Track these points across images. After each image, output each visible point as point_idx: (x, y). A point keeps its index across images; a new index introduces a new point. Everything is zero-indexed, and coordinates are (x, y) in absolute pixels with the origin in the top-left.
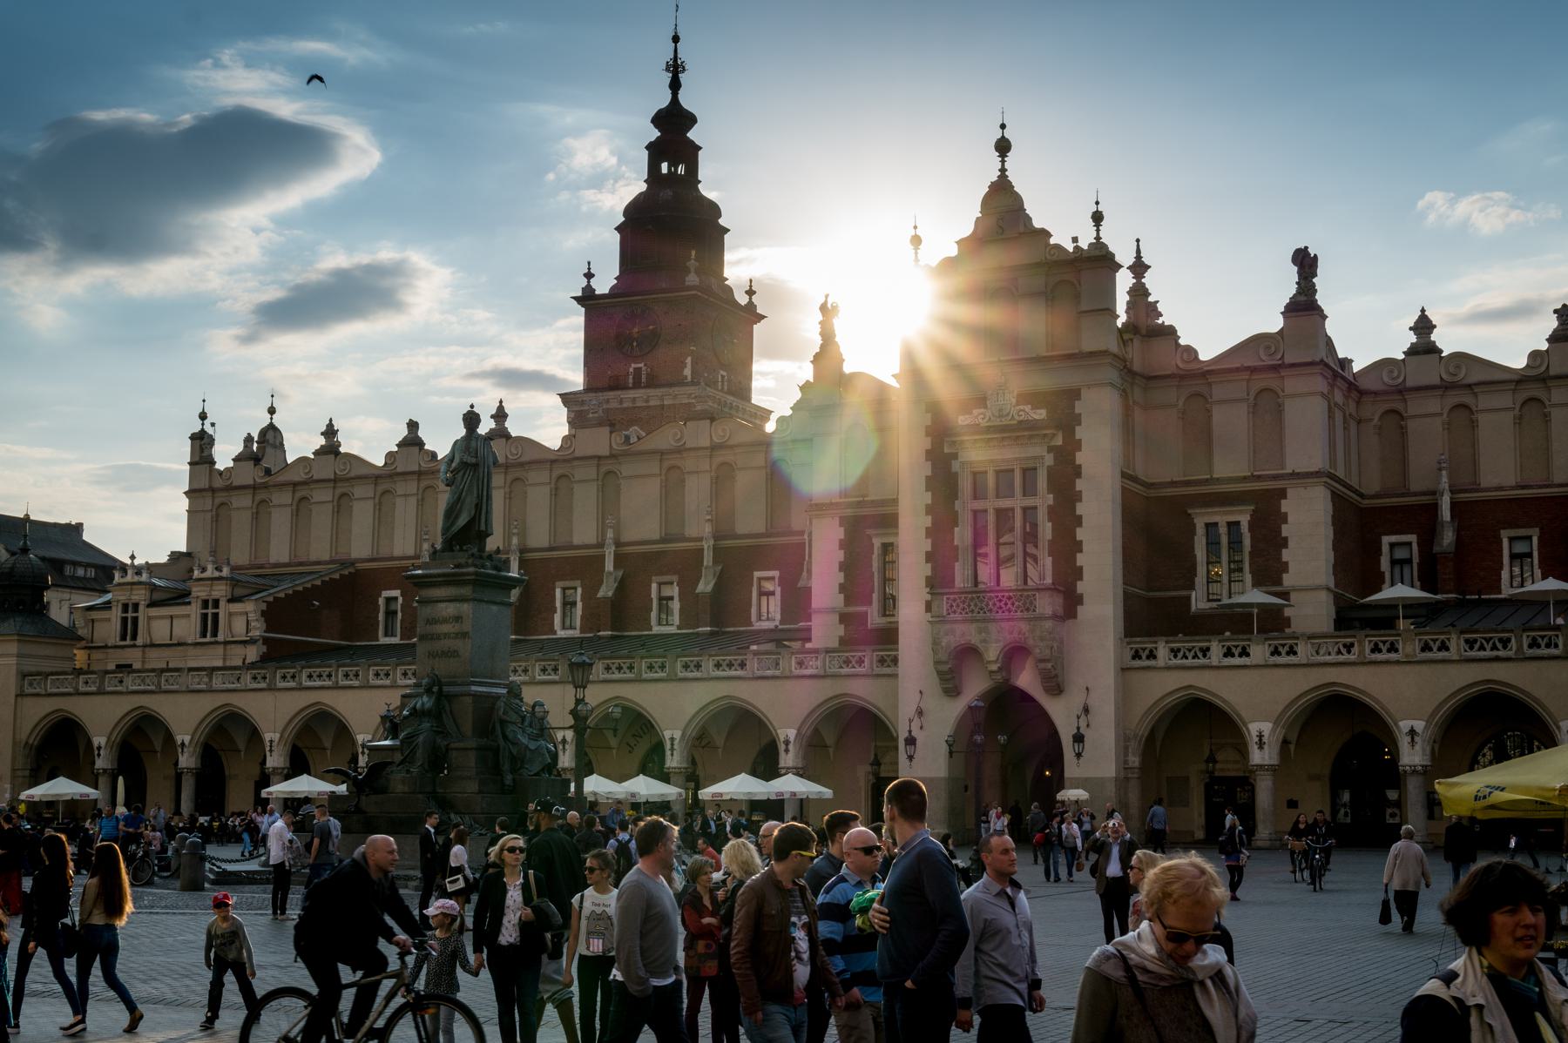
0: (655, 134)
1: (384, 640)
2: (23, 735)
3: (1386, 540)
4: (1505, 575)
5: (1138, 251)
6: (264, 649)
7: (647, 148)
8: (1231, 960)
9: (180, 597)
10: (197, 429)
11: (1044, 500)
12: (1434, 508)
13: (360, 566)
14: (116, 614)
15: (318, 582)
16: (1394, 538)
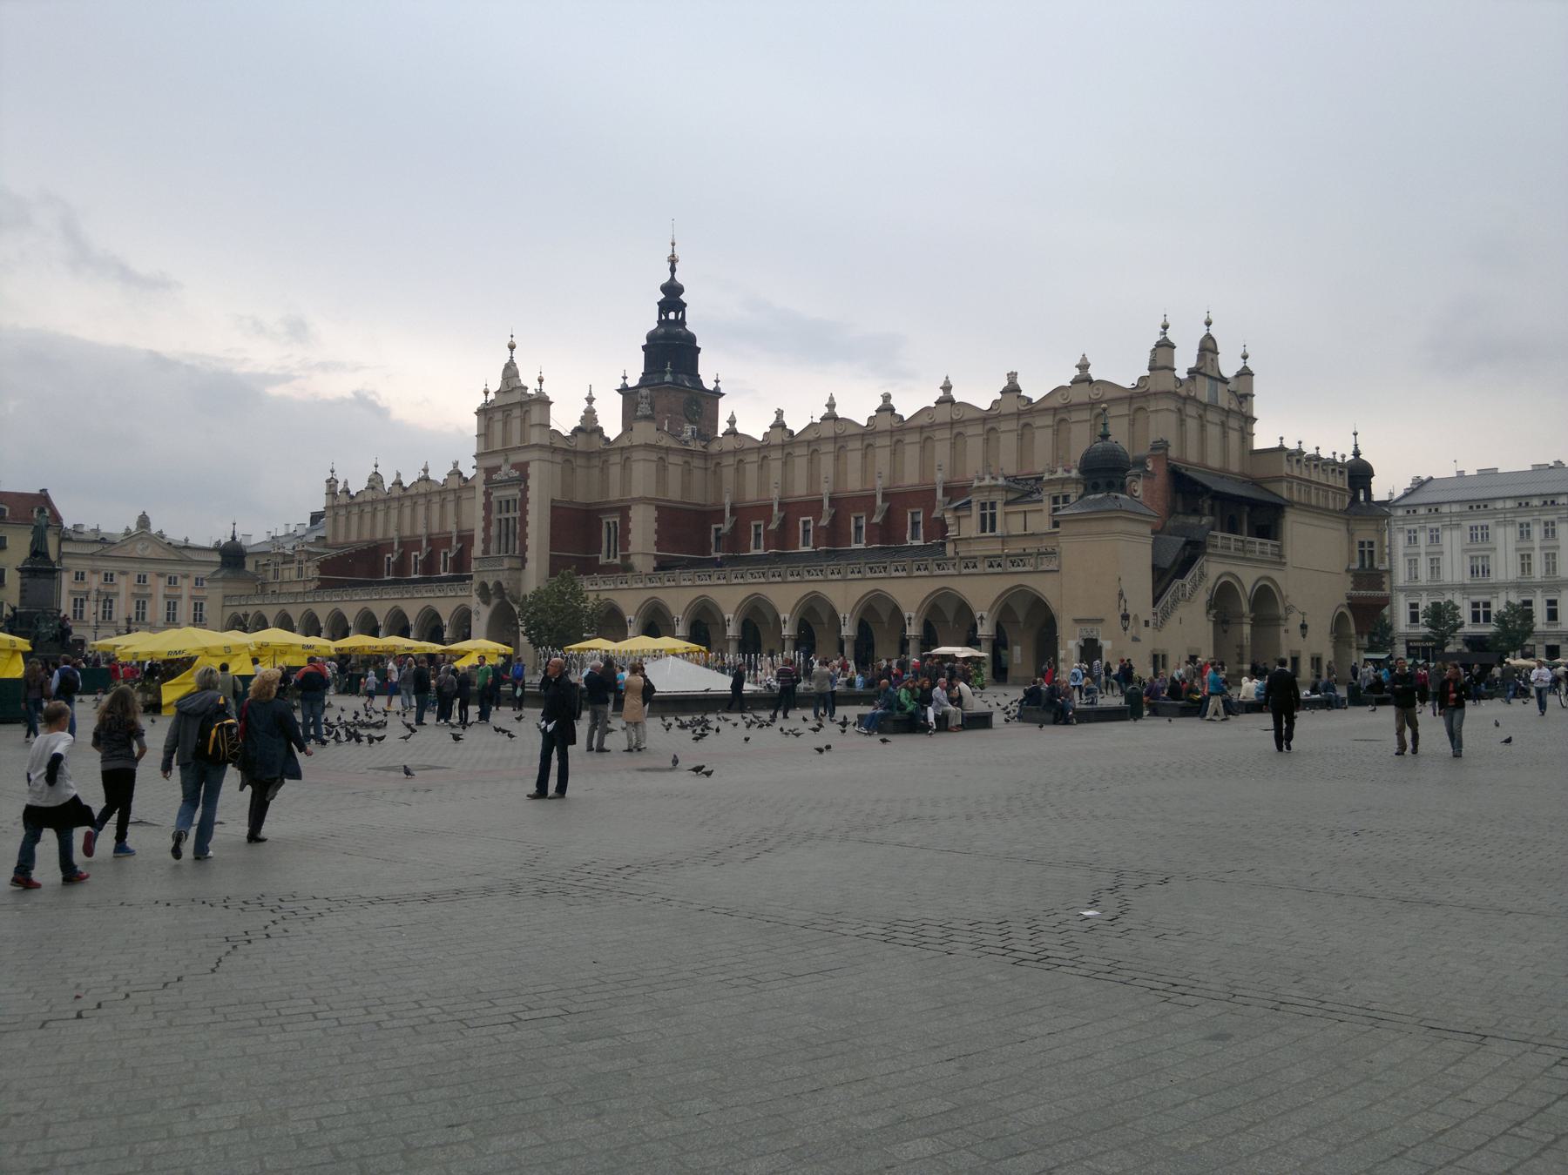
0: (664, 296)
1: (387, 578)
2: (224, 624)
3: (714, 526)
4: (752, 543)
5: (590, 391)
6: (319, 583)
7: (659, 303)
8: (403, 722)
9: (293, 562)
10: (330, 477)
11: (518, 514)
12: (724, 510)
13: (379, 542)
14: (272, 567)
15: (353, 551)
16: (805, 519)
